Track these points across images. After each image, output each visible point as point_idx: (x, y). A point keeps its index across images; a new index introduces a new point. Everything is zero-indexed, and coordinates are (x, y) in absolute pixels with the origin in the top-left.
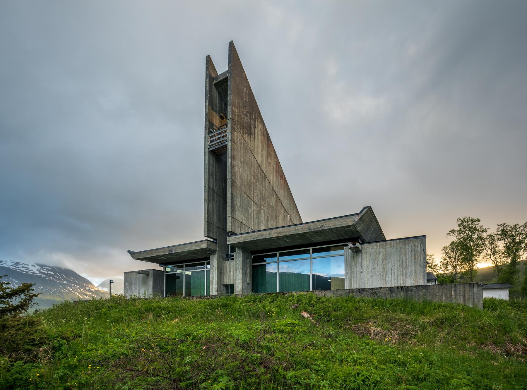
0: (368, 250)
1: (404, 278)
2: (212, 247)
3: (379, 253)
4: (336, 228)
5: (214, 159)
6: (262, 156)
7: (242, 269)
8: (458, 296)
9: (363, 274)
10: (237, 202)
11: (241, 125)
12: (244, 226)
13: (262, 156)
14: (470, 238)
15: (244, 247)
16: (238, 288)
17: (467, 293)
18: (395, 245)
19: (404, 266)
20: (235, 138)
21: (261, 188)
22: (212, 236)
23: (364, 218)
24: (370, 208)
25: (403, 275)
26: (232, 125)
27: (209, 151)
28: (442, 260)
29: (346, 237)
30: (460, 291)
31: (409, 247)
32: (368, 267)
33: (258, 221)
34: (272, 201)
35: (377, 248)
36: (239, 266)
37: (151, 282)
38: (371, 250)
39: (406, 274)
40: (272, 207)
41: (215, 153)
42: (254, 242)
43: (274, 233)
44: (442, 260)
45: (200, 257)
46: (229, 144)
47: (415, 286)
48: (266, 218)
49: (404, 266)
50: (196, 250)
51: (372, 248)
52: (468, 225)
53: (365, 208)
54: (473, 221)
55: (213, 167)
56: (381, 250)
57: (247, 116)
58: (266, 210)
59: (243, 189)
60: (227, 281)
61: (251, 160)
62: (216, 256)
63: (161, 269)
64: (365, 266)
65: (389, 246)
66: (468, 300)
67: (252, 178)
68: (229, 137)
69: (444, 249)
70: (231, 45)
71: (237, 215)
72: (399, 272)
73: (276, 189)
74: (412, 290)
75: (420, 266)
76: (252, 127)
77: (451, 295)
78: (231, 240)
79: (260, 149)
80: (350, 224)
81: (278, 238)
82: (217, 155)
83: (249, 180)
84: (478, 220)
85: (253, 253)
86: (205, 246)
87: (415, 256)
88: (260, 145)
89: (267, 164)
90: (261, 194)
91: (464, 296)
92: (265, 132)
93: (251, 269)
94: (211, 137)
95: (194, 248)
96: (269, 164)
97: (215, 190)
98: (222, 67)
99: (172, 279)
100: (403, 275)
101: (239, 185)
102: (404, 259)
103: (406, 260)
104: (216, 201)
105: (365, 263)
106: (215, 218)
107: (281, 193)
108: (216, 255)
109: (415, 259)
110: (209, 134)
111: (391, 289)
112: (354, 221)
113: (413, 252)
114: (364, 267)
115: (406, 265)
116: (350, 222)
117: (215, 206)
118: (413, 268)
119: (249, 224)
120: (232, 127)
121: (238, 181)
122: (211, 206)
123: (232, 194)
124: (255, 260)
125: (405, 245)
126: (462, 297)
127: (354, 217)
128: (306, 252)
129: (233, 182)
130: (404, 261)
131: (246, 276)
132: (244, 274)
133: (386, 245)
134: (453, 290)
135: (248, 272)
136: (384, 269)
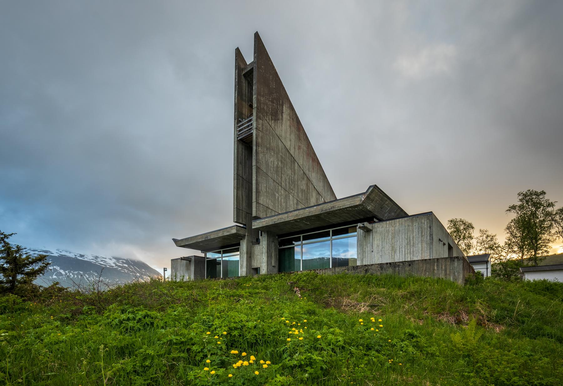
0: (378, 229)
1: (412, 256)
2: (241, 232)
3: (388, 231)
4: (346, 208)
5: (243, 148)
6: (291, 141)
7: (267, 253)
8: (441, 271)
9: (373, 253)
10: (263, 187)
11: (267, 112)
12: (270, 211)
13: (291, 141)
14: (534, 214)
15: (269, 230)
16: (264, 270)
17: (448, 267)
18: (403, 223)
19: (412, 244)
20: (260, 126)
21: (289, 172)
22: (241, 221)
23: (371, 197)
24: (375, 187)
25: (410, 253)
26: (257, 114)
27: (238, 141)
28: (507, 241)
29: (362, 217)
30: (442, 265)
31: (416, 224)
32: (378, 246)
33: (286, 205)
34: (303, 185)
35: (386, 227)
36: (265, 250)
37: (192, 268)
38: (381, 230)
39: (413, 252)
40: (303, 191)
41: (244, 142)
42: (275, 226)
43: (292, 216)
44: (507, 241)
45: (235, 243)
46: (254, 132)
47: (402, 262)
48: (295, 201)
49: (412, 244)
50: (227, 236)
51: (382, 227)
52: (532, 199)
53: (370, 187)
54: (537, 194)
55: (242, 155)
56: (390, 229)
57: (273, 103)
58: (295, 194)
59: (269, 174)
60: (255, 265)
61: (278, 146)
62: (245, 241)
63: (203, 255)
64: (376, 246)
65: (398, 224)
66: (449, 275)
67: (280, 163)
68: (254, 125)
69: (509, 228)
70: (257, 36)
71: (262, 200)
72: (406, 250)
73: (307, 172)
74: (399, 265)
75: (427, 244)
76: (279, 112)
77: (434, 269)
78: (256, 225)
79: (288, 133)
80: (357, 204)
81: (295, 220)
82: (246, 143)
83: (275, 165)
84: (543, 193)
85: (280, 236)
86: (234, 231)
87: (422, 233)
88: (289, 130)
89: (297, 148)
90: (289, 178)
91: (446, 271)
92: (294, 116)
93: (277, 253)
94: (239, 127)
95: (226, 234)
96: (299, 148)
97: (244, 177)
98: (249, 58)
99: (213, 264)
100: (410, 253)
101: (265, 171)
102: (411, 236)
103: (413, 237)
104: (246, 188)
105: (376, 243)
106: (244, 204)
107: (314, 176)
108: (246, 240)
109: (422, 236)
110: (238, 123)
111: (381, 266)
112: (361, 200)
113: (420, 229)
114: (375, 246)
115: (413, 243)
116: (357, 202)
117: (243, 193)
118: (420, 246)
119: (279, 207)
120: (257, 116)
121: (263, 168)
122: (240, 193)
123: (257, 180)
124: (281, 243)
125: (412, 223)
126: (443, 272)
127: (361, 196)
128: (327, 234)
129: (258, 168)
130: (411, 238)
131: (271, 259)
132: (269, 257)
133: (395, 224)
134: (436, 264)
135: (273, 255)
136: (393, 247)
